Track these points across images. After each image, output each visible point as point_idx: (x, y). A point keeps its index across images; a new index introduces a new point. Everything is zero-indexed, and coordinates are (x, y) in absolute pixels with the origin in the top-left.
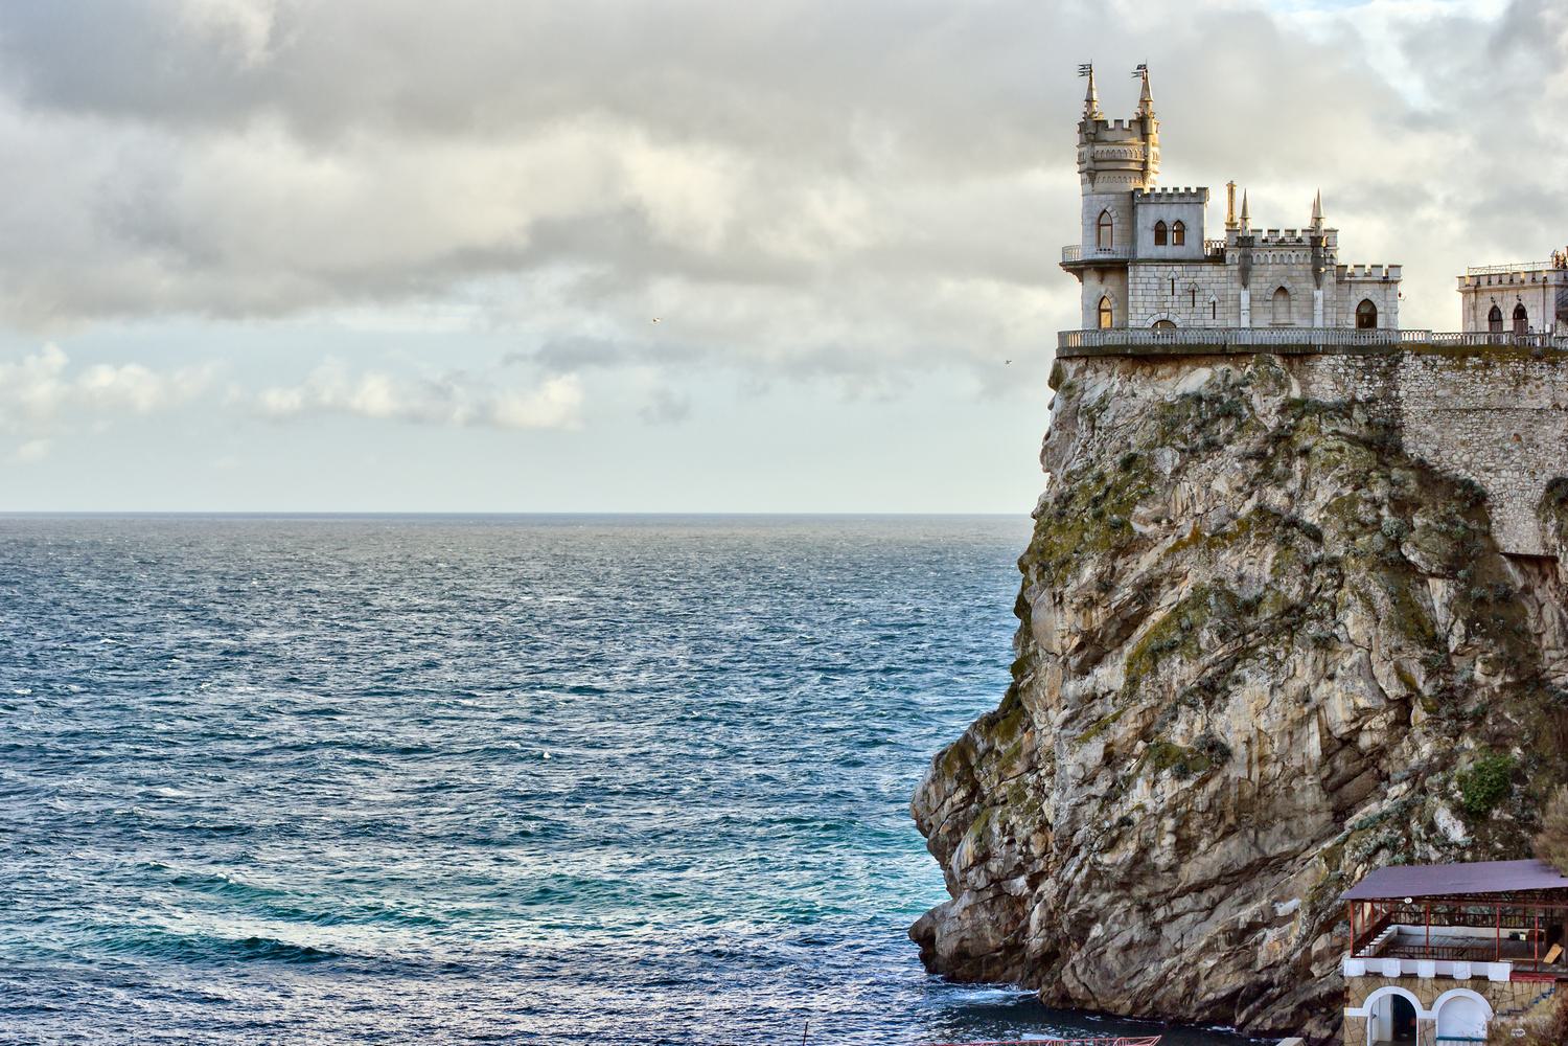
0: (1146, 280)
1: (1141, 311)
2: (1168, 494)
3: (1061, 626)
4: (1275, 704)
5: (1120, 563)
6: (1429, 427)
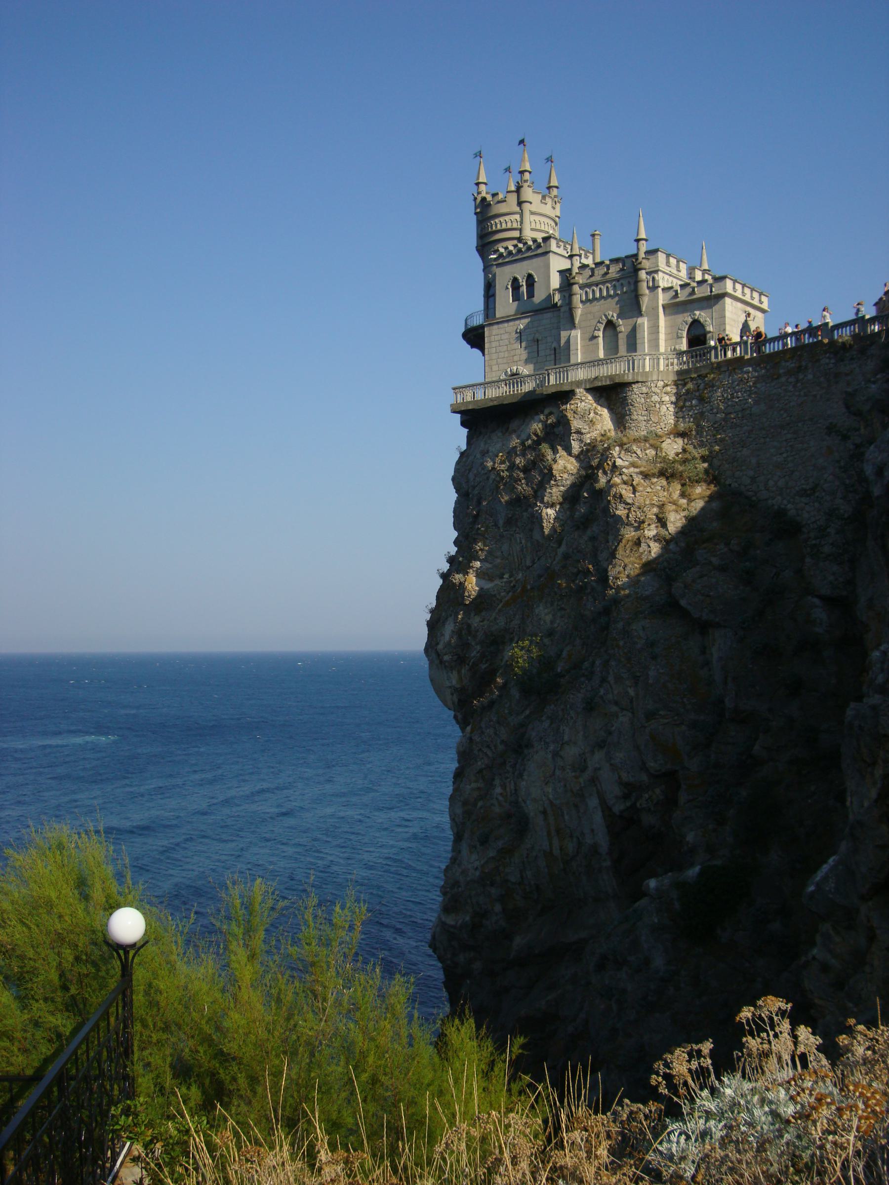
0: (497, 338)
1: (495, 368)
2: (505, 547)
3: (448, 684)
4: (558, 772)
5: (475, 621)
6: (745, 452)
